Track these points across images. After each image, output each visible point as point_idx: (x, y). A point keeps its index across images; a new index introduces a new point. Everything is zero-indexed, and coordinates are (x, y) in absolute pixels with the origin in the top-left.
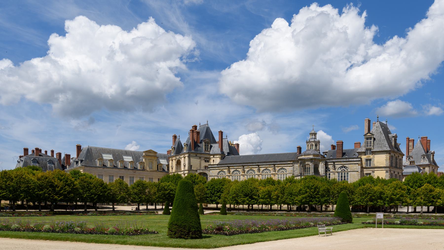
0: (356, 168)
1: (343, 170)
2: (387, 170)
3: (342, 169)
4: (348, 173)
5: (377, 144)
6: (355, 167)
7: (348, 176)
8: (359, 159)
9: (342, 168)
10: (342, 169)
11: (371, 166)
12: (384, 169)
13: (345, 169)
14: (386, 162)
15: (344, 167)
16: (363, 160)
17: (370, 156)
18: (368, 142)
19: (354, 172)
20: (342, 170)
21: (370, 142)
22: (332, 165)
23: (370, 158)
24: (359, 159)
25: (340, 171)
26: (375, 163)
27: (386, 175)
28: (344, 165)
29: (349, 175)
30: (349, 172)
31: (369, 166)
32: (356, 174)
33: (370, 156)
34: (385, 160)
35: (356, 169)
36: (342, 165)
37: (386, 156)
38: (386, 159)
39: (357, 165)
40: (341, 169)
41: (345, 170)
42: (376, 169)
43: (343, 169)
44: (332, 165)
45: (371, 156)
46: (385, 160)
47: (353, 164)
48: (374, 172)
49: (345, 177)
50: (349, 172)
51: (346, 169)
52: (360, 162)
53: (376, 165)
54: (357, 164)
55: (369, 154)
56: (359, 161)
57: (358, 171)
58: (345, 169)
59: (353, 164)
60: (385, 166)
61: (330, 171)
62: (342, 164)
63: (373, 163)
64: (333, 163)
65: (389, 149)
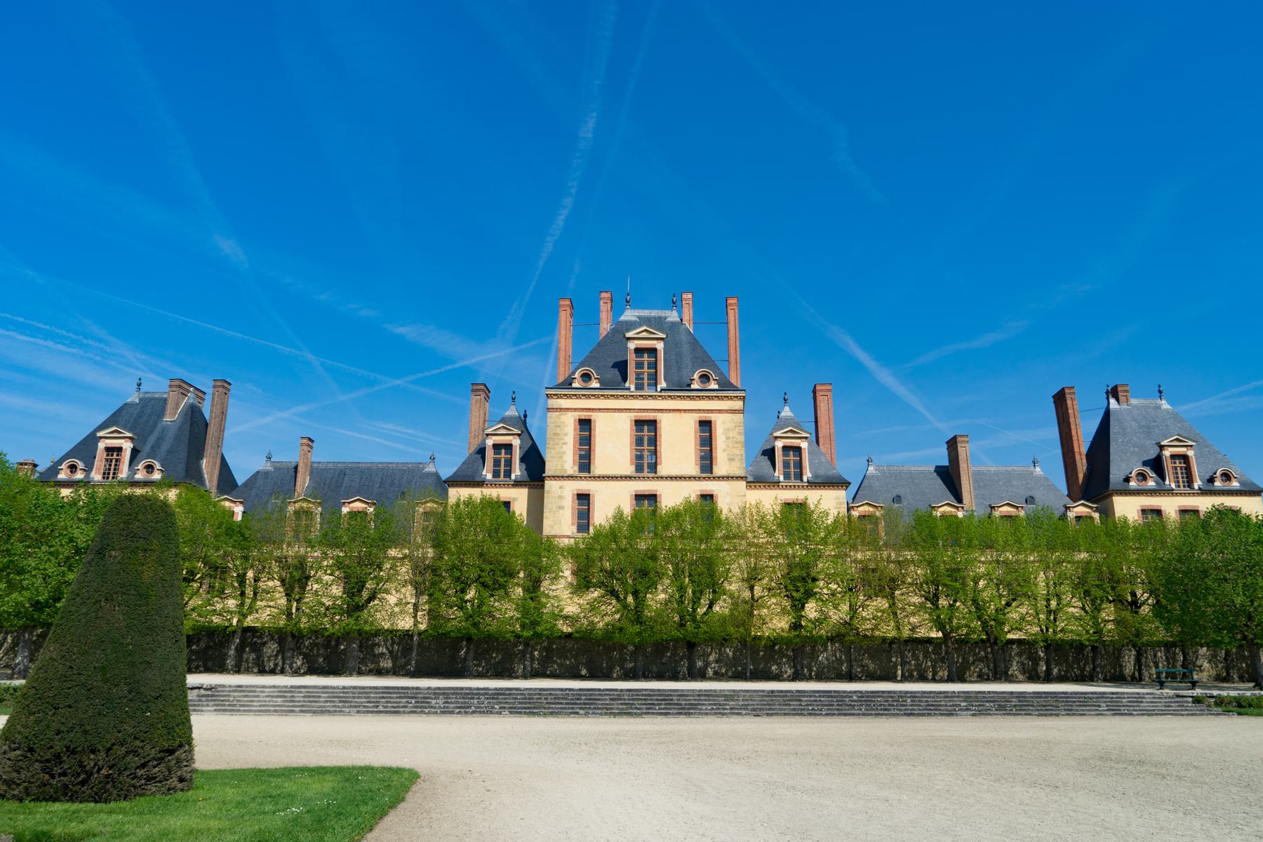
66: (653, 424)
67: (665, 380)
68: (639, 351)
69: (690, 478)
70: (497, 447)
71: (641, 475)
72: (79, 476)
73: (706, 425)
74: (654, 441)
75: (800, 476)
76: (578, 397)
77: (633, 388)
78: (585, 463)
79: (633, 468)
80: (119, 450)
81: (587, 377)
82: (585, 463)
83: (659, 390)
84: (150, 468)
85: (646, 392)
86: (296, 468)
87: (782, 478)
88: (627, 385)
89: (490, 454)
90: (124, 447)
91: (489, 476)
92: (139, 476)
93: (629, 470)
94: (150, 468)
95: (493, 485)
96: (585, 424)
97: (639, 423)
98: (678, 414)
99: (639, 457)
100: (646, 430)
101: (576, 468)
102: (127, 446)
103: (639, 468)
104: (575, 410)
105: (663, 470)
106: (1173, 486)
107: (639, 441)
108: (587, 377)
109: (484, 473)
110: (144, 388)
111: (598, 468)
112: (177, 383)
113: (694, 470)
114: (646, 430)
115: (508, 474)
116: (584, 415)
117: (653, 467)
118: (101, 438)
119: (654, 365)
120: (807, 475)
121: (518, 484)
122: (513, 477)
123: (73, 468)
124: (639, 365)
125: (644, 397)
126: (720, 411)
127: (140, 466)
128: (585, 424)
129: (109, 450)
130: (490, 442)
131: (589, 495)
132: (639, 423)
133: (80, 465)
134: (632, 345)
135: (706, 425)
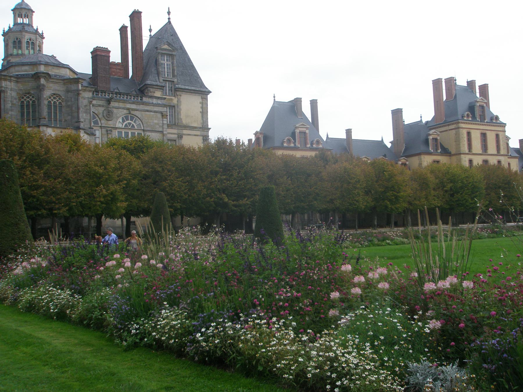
0: (158, 124)
1: (130, 124)
3: (127, 122)
6: (156, 121)
10: (127, 122)
12: (198, 133)
13: (133, 123)
17: (172, 100)
20: (126, 125)
23: (172, 105)
25: (123, 127)
33: (172, 100)
35: (157, 126)
40: (125, 123)
41: (133, 126)
42: (185, 132)
43: (129, 121)
44: (103, 106)
54: (162, 113)
58: (133, 123)
59: (151, 111)
62: (128, 109)
72: (292, 145)
114: (484, 136)
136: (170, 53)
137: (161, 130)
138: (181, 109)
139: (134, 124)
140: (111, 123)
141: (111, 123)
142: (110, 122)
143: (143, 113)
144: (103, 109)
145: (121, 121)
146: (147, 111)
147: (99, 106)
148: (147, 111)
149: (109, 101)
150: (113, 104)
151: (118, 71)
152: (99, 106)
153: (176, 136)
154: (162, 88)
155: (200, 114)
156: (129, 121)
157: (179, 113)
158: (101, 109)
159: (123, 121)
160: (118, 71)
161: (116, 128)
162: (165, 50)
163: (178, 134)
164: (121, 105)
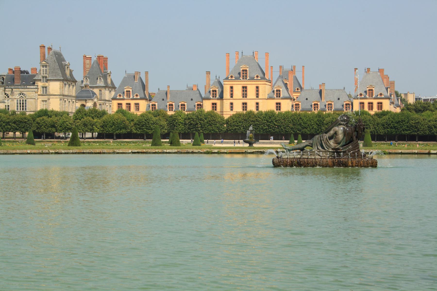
0: (33, 96)
1: (21, 96)
2: (61, 98)
3: (20, 96)
4: (26, 101)
5: (52, 73)
6: (32, 95)
7: (26, 103)
8: (36, 87)
9: (21, 95)
10: (20, 96)
11: (46, 93)
12: (58, 97)
13: (23, 96)
14: (60, 90)
15: (23, 94)
16: (39, 87)
18: (44, 70)
19: (31, 100)
20: (20, 97)
21: (45, 70)
22: (10, 91)
23: (46, 86)
24: (36, 87)
26: (50, 91)
27: (60, 103)
28: (22, 92)
29: (27, 102)
30: (27, 99)
31: (45, 93)
32: (33, 101)
33: (45, 84)
34: (59, 88)
35: (33, 97)
36: (20, 92)
37: (60, 84)
38: (59, 87)
39: (34, 92)
40: (20, 96)
41: (23, 97)
42: (51, 97)
43: (22, 95)
44: (10, 91)
45: (47, 84)
46: (59, 88)
47: (30, 91)
48: (50, 99)
49: (23, 104)
50: (27, 99)
51: (24, 96)
52: (37, 90)
53: (51, 93)
54: (35, 91)
55: (45, 82)
56: (36, 88)
57: (35, 99)
58: (23, 96)
59: (30, 91)
60: (59, 94)
61: (9, 97)
62: (20, 91)
63: (49, 91)
64: (11, 90)
65: (62, 78)
66: (246, 87)
67: (249, 77)
68: (243, 71)
69: (255, 99)
70: (213, 91)
71: (243, 98)
72: (122, 97)
73: (257, 87)
74: (246, 91)
75: (280, 96)
76: (230, 81)
77: (242, 79)
78: (232, 96)
79: (242, 97)
80: (129, 91)
81: (232, 77)
82: (232, 96)
83: (247, 79)
84: (137, 96)
85: (245, 80)
86: (167, 92)
87: (276, 97)
88: (240, 78)
89: (211, 92)
90: (130, 91)
91: (212, 97)
92: (135, 97)
93: (241, 97)
94: (137, 96)
95: (212, 99)
96: (232, 88)
97: (243, 87)
98: (251, 85)
99: (243, 94)
100: (245, 89)
101: (230, 97)
102: (131, 90)
103: (243, 97)
104: (229, 84)
105: (248, 97)
106: (368, 97)
107: (243, 91)
108: (232, 77)
109: (210, 97)
110: (127, 73)
111: (234, 97)
112: (137, 73)
113: (255, 97)
114: (245, 89)
115: (216, 97)
116: (231, 85)
117: (246, 97)
118: (125, 89)
119: (246, 73)
120: (281, 96)
121: (218, 99)
122: (217, 97)
123: (120, 96)
124: (243, 73)
125: (244, 81)
126: (260, 84)
127: (135, 95)
128: (232, 88)
129: (127, 91)
130: (211, 90)
131: (233, 103)
132: (243, 87)
133: (122, 95)
134: (242, 69)
135: (257, 87)
136: (46, 65)
137: (34, 98)
138: (49, 88)
139: (23, 96)
140: (13, 97)
141: (13, 97)
142: (13, 97)
143: (27, 92)
144: (11, 92)
145: (18, 95)
146: (28, 91)
147: (9, 91)
148: (28, 91)
149: (12, 89)
150: (14, 90)
151: (34, 71)
152: (9, 91)
153: (47, 99)
154: (40, 80)
155: (59, 89)
156: (22, 95)
157: (49, 89)
158: (10, 92)
159: (19, 95)
160: (34, 71)
161: (16, 99)
162: (43, 64)
163: (48, 98)
164: (18, 90)
